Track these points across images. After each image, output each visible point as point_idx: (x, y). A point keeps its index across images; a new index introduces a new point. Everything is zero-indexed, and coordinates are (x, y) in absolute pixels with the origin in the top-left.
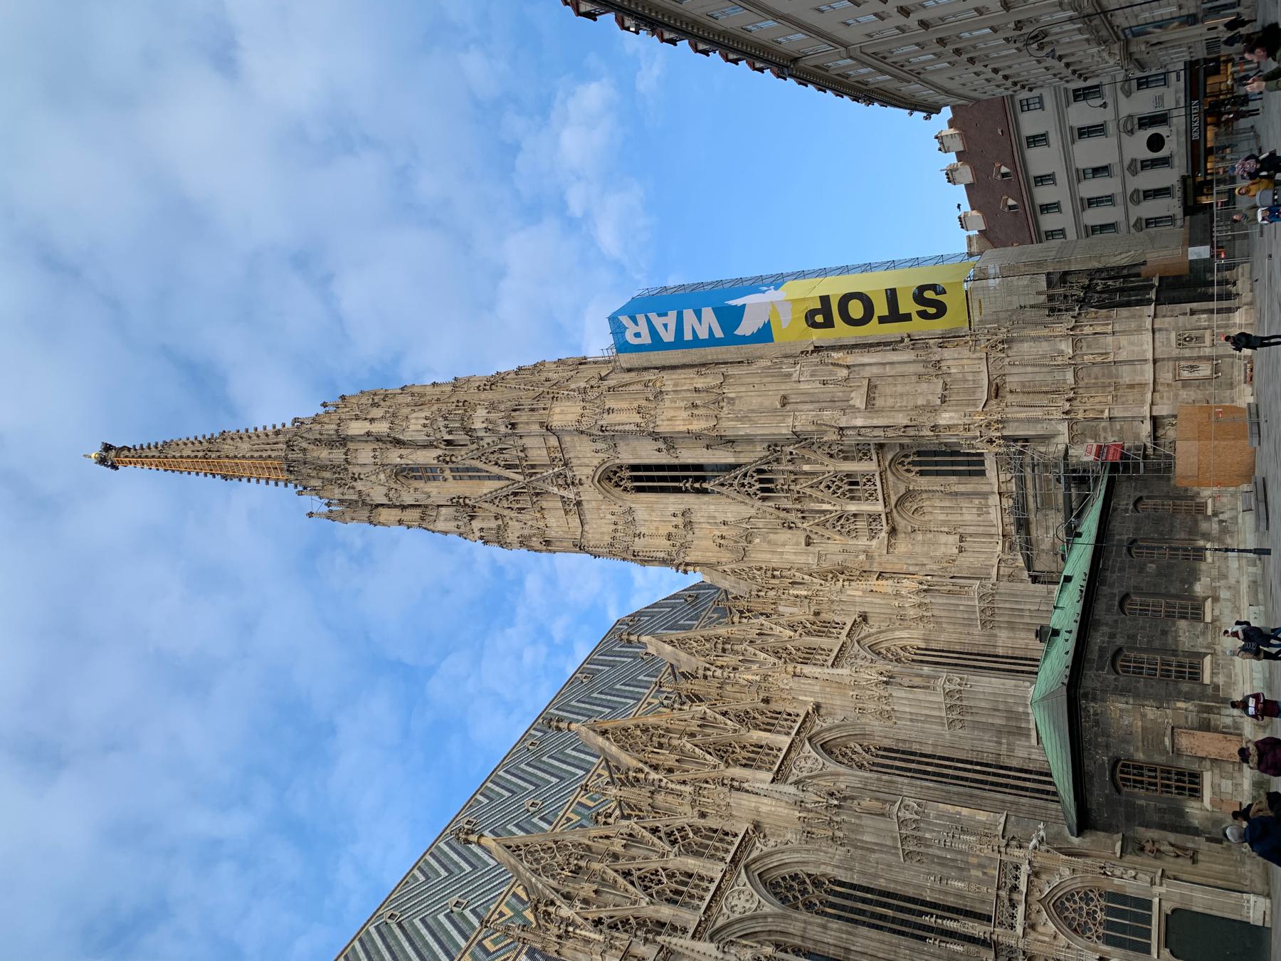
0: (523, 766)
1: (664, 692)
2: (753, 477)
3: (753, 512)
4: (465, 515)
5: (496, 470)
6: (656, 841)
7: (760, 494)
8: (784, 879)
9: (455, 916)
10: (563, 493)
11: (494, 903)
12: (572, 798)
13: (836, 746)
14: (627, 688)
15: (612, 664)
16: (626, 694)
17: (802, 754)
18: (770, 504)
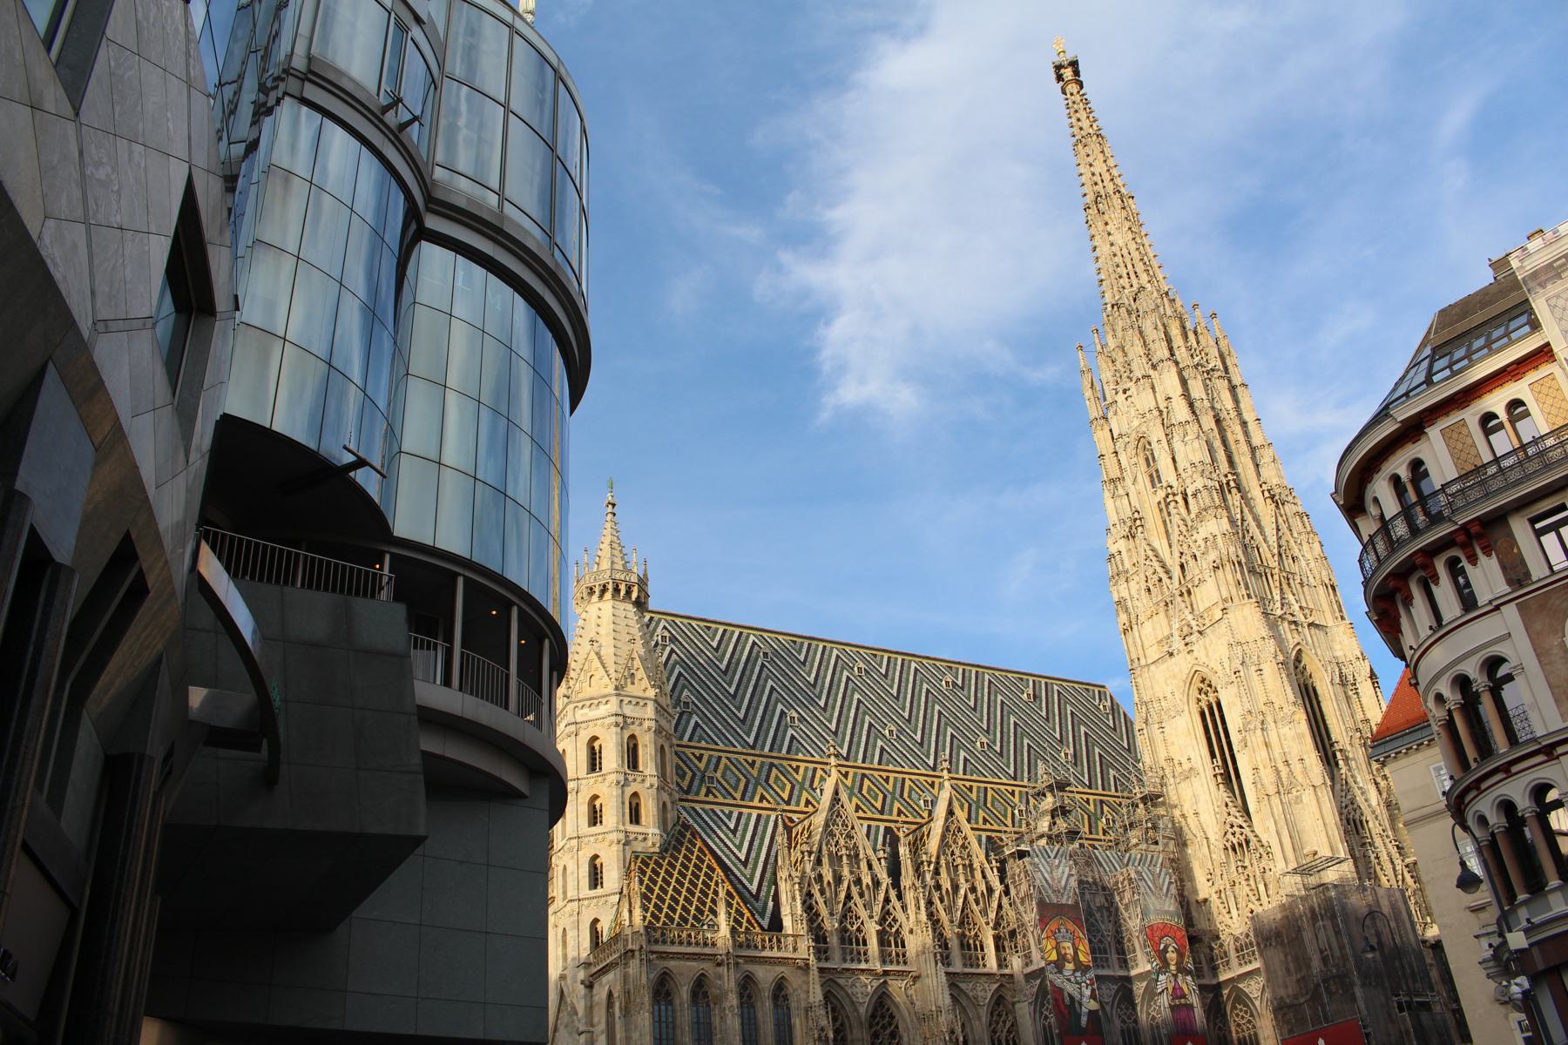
0: (925, 686)
1: (1028, 802)
2: (1242, 834)
3: (1212, 840)
4: (1127, 530)
5: (1177, 555)
6: (880, 906)
7: (1229, 845)
8: (888, 1009)
9: (783, 723)
10: (1176, 633)
11: (804, 755)
12: (907, 769)
13: (1005, 1006)
14: (1026, 754)
15: (1051, 716)
16: (1019, 758)
17: (986, 985)
18: (1223, 857)
